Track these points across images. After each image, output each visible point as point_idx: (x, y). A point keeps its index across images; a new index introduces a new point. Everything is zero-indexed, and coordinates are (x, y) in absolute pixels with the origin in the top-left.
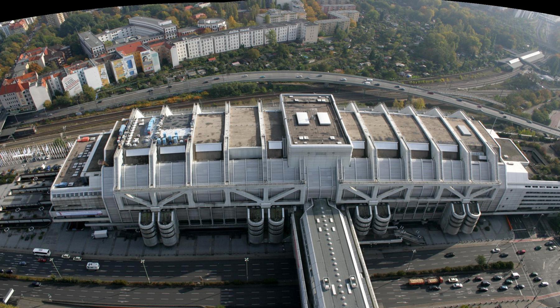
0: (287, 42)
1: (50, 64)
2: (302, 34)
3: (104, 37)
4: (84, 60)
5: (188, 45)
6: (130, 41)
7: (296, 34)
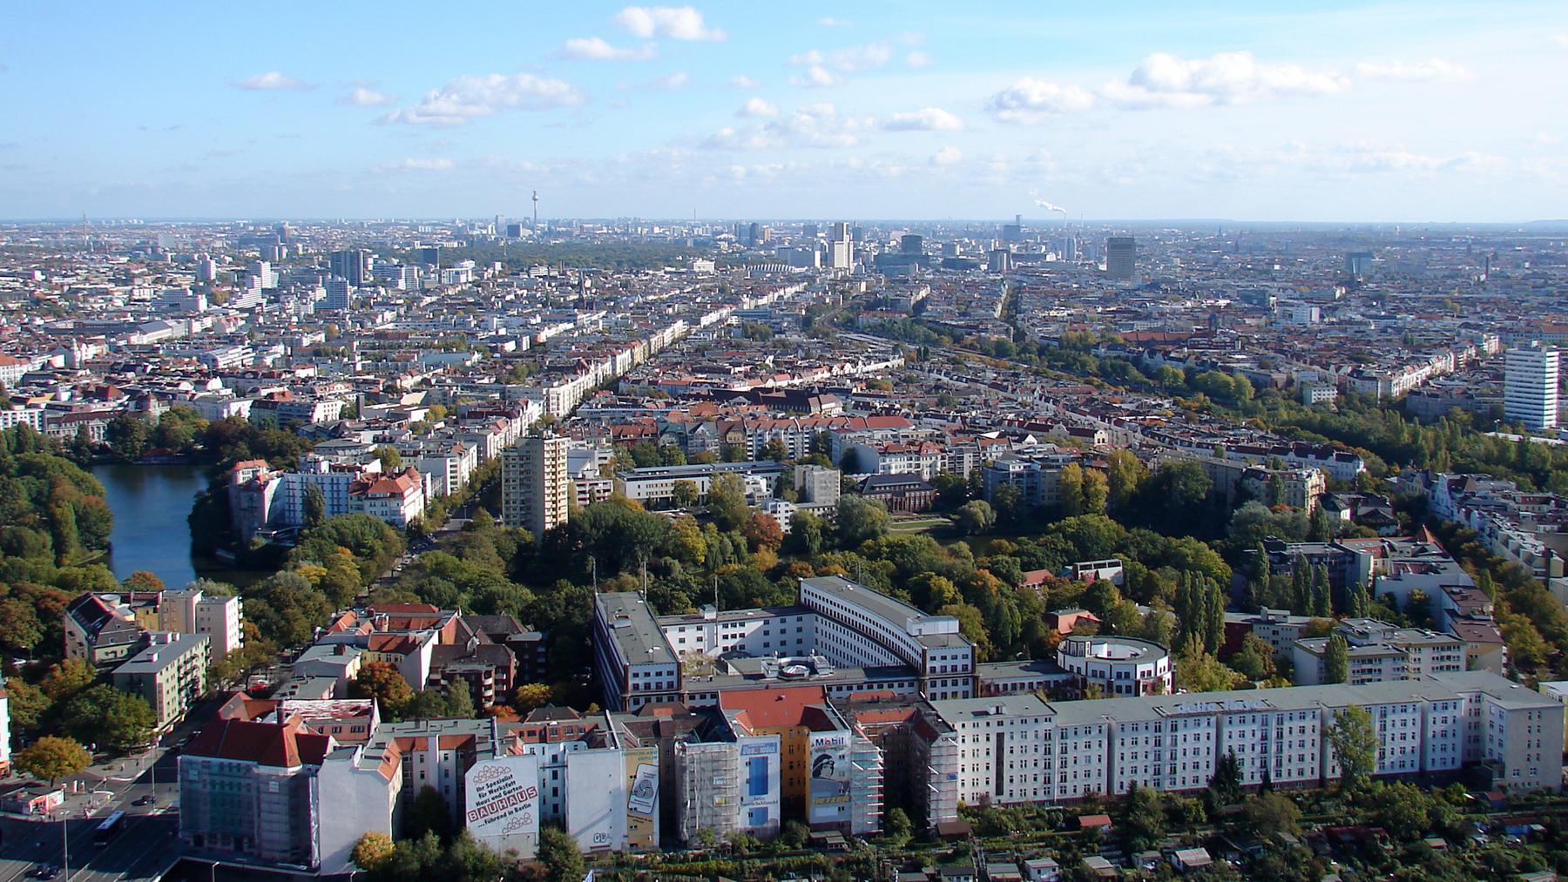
0: (1423, 779)
1: (444, 687)
2: (1488, 745)
3: (691, 633)
4: (583, 708)
5: (1007, 738)
6: (783, 676)
7: (1459, 741)
